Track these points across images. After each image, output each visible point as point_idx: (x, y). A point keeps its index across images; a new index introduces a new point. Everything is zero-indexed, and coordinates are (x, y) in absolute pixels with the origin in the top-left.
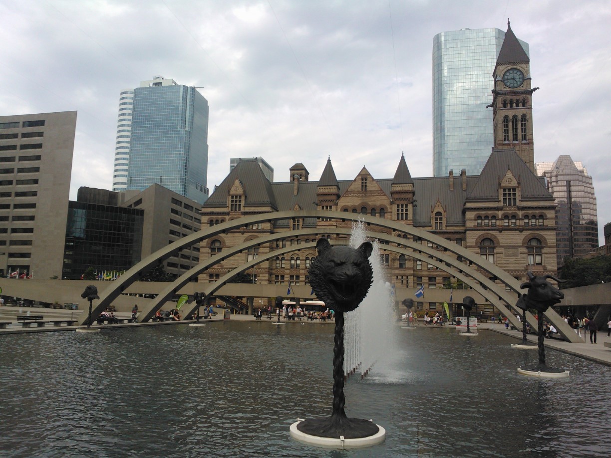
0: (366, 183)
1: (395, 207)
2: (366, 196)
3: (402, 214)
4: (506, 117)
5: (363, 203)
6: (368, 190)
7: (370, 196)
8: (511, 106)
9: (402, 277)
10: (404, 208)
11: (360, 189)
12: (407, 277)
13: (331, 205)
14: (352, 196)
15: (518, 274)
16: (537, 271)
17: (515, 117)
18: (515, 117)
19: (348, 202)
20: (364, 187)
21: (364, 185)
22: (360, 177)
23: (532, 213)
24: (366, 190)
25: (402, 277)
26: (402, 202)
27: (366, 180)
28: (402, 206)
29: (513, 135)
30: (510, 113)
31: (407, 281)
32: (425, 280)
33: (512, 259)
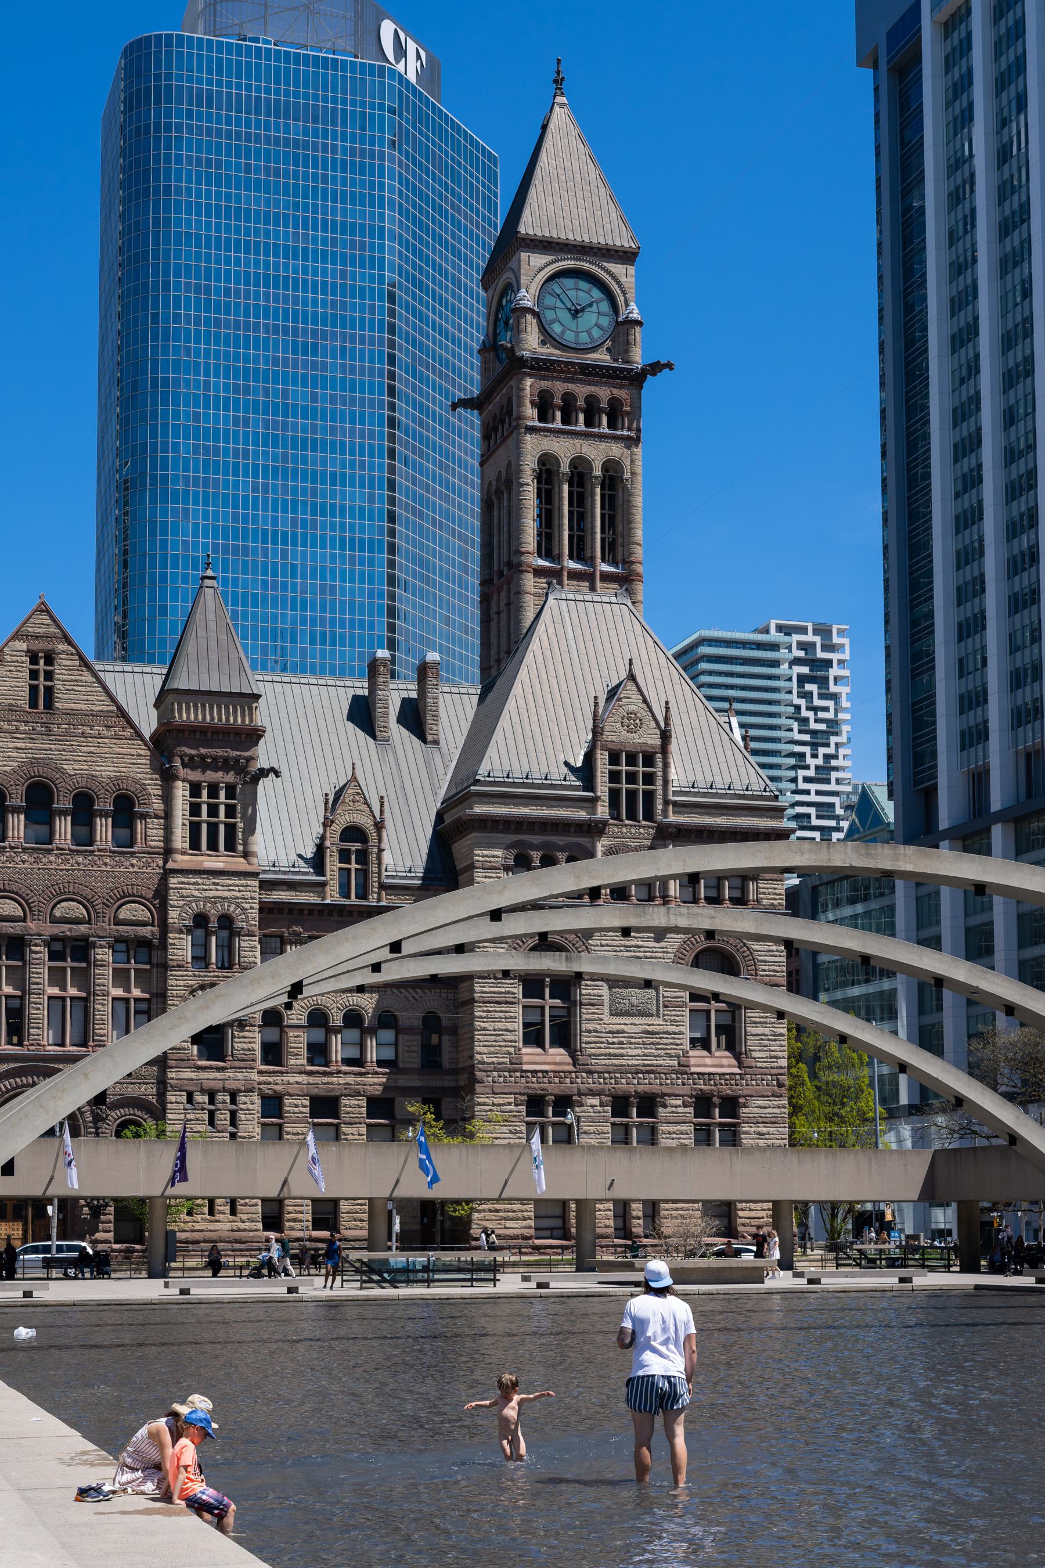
0: (49, 676)
1: (181, 792)
2: (49, 732)
5: (33, 762)
11: (24, 703)
21: (42, 682)
24: (49, 704)
27: (49, 660)
28: (213, 792)
32: (297, 1107)
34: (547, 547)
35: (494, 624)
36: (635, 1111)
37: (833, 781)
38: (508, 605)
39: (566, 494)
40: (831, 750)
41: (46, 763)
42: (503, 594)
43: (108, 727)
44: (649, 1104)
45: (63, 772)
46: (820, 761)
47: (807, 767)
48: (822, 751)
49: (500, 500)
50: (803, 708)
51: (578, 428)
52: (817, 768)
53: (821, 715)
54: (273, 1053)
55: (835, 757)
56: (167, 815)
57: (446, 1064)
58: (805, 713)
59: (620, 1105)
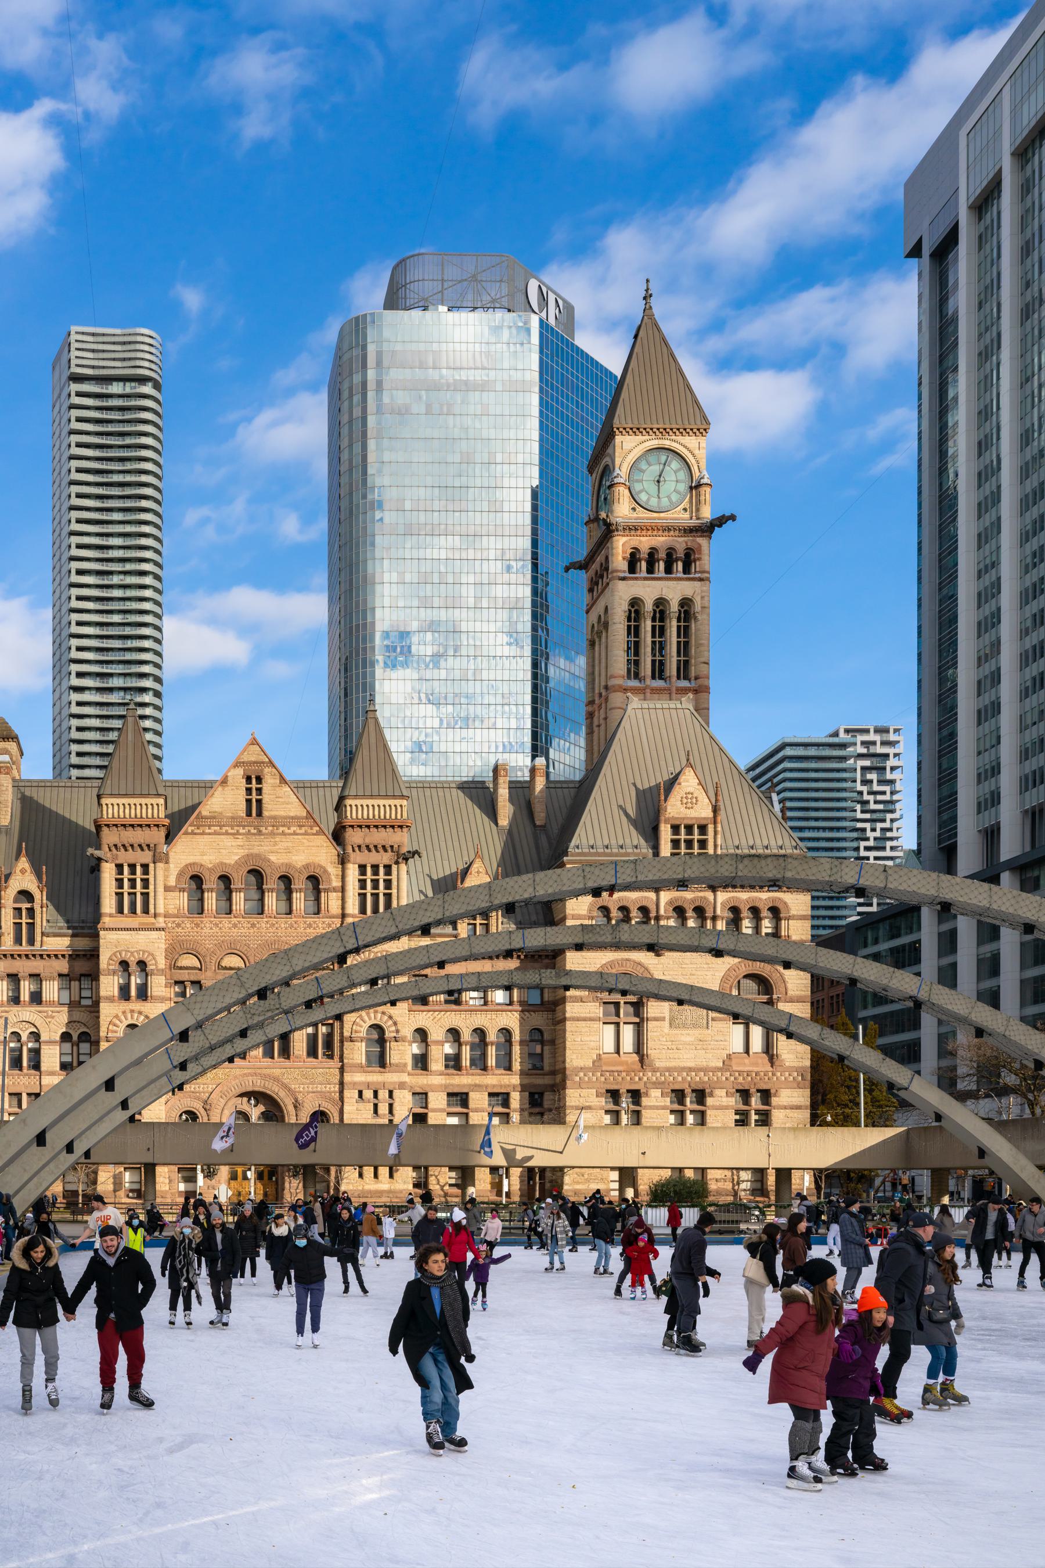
0: (259, 791)
1: (353, 873)
2: (260, 833)
3: (376, 896)
4: (635, 603)
6: (265, 813)
7: (272, 834)
8: (650, 570)
9: (376, 1093)
10: (382, 876)
12: (391, 1093)
13: (145, 861)
14: (215, 833)
15: (706, 1079)
16: (756, 1069)
17: (661, 604)
18: (661, 604)
19: (203, 854)
20: (255, 808)
21: (254, 797)
22: (240, 772)
23: (693, 900)
24: (260, 814)
25: (376, 1093)
26: (374, 858)
27: (259, 780)
29: (653, 662)
30: (647, 590)
31: (391, 1106)
33: (688, 1036)
34: (634, 670)
35: (596, 735)
36: (690, 1100)
37: (888, 848)
38: (606, 719)
39: (649, 629)
40: (887, 825)
41: (258, 856)
42: (602, 711)
43: (300, 826)
44: (701, 1096)
45: (269, 861)
46: (878, 834)
47: (867, 839)
48: (879, 825)
49: (600, 637)
50: (865, 793)
51: (660, 575)
52: (875, 839)
53: (879, 797)
54: (422, 1062)
55: (890, 830)
56: (343, 889)
57: (547, 1068)
58: (866, 797)
59: (679, 1095)
